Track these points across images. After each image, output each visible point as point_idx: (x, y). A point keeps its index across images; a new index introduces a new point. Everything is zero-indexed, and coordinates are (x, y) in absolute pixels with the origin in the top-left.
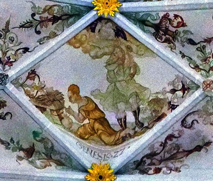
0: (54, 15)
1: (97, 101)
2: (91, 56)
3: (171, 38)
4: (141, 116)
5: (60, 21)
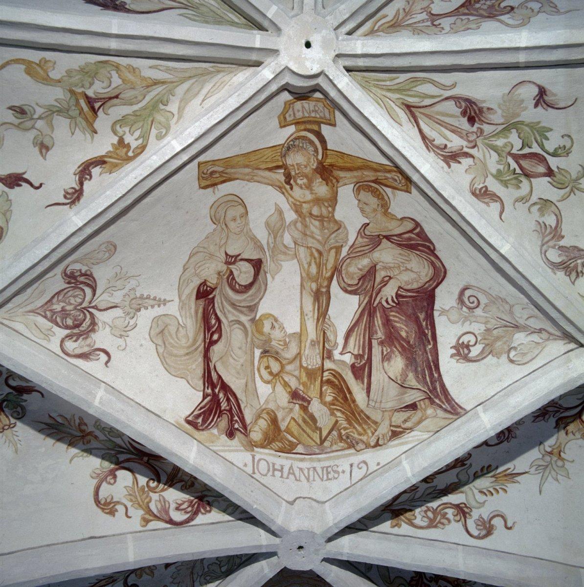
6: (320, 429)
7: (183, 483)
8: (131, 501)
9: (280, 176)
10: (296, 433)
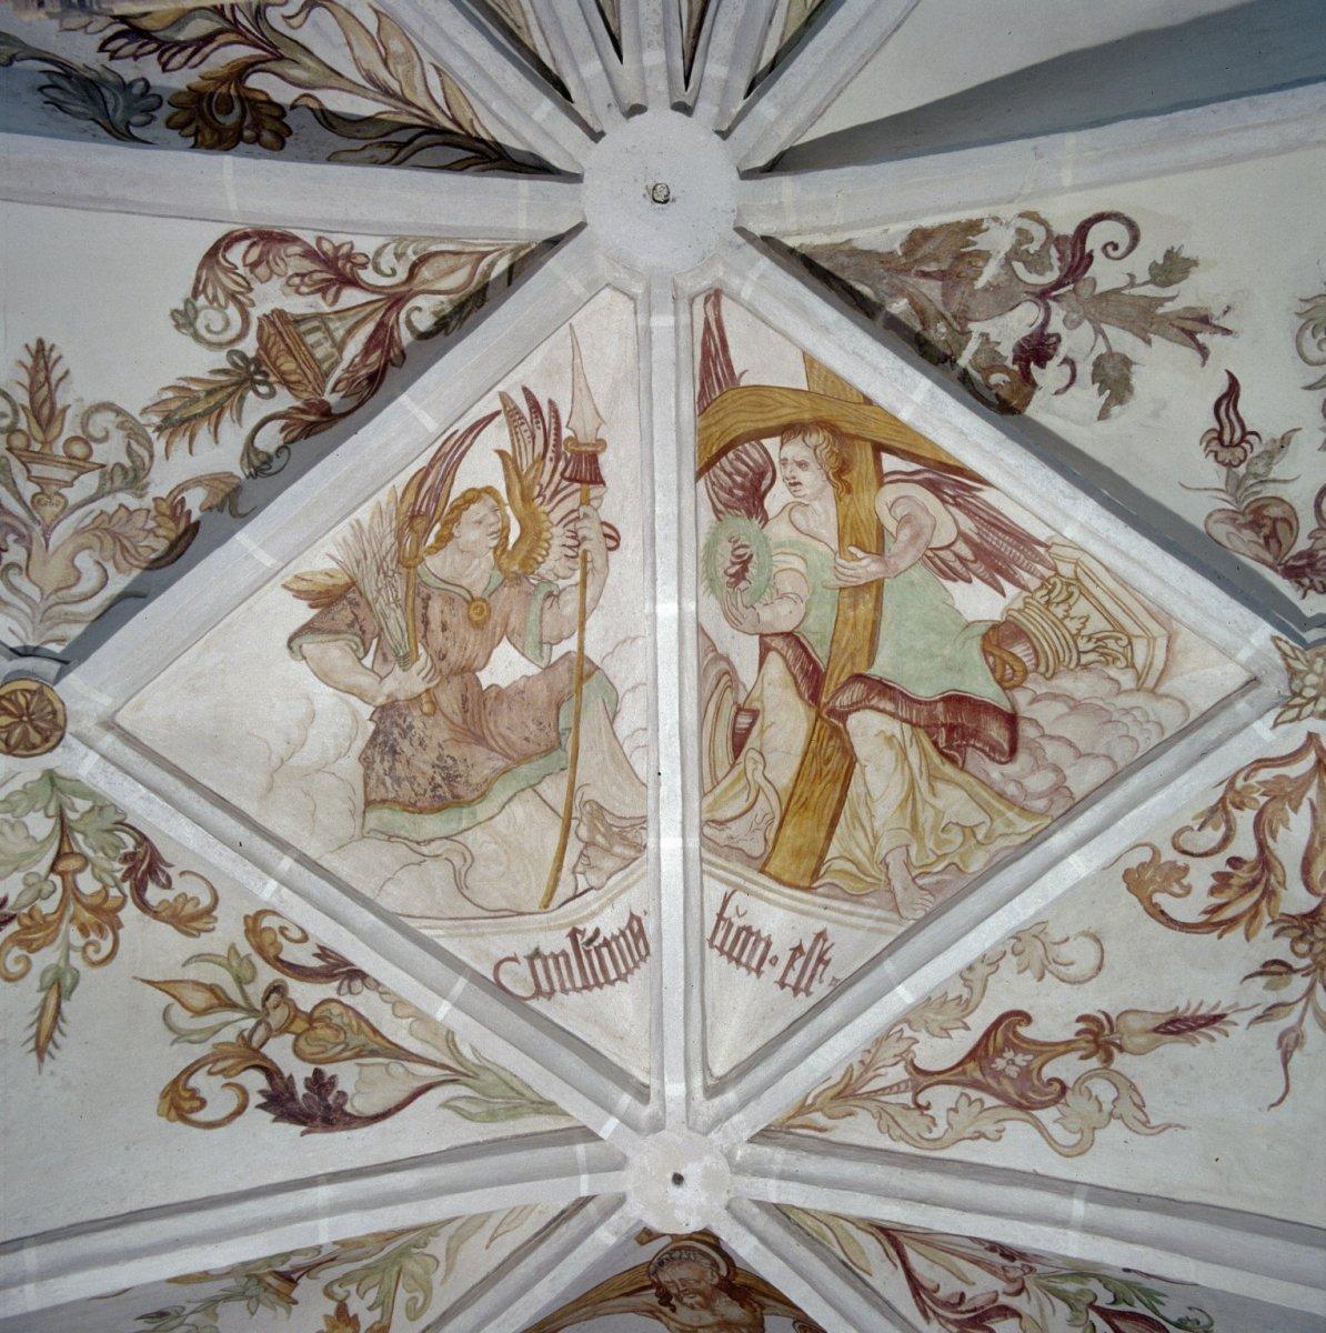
9: (650, 1297)
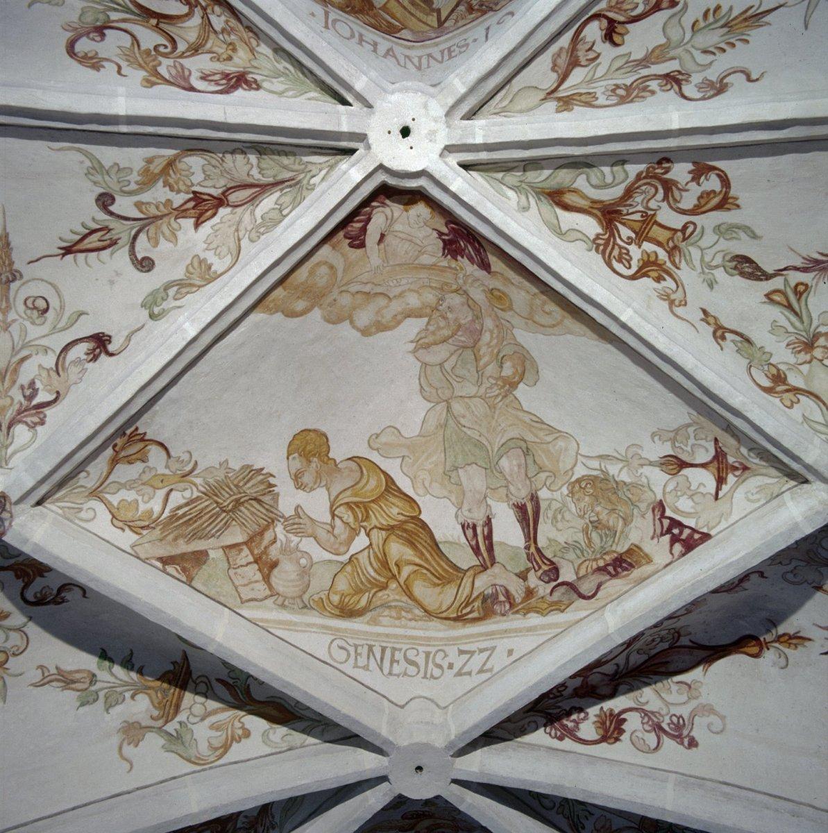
0: (194, 193)
1: (392, 467)
2: (358, 329)
3: (662, 255)
4: (545, 532)
5: (223, 211)
6: (439, 11)
7: (215, 55)
8: (128, 61)
10: (398, 15)
